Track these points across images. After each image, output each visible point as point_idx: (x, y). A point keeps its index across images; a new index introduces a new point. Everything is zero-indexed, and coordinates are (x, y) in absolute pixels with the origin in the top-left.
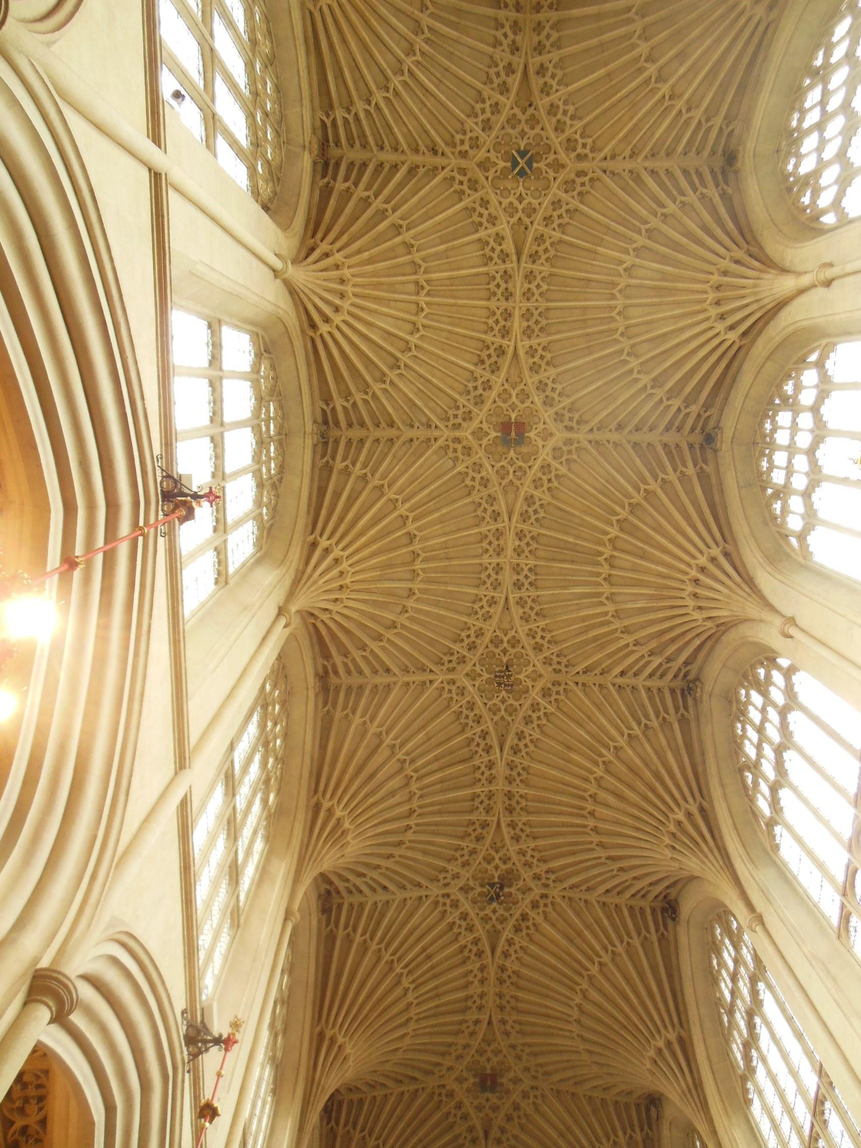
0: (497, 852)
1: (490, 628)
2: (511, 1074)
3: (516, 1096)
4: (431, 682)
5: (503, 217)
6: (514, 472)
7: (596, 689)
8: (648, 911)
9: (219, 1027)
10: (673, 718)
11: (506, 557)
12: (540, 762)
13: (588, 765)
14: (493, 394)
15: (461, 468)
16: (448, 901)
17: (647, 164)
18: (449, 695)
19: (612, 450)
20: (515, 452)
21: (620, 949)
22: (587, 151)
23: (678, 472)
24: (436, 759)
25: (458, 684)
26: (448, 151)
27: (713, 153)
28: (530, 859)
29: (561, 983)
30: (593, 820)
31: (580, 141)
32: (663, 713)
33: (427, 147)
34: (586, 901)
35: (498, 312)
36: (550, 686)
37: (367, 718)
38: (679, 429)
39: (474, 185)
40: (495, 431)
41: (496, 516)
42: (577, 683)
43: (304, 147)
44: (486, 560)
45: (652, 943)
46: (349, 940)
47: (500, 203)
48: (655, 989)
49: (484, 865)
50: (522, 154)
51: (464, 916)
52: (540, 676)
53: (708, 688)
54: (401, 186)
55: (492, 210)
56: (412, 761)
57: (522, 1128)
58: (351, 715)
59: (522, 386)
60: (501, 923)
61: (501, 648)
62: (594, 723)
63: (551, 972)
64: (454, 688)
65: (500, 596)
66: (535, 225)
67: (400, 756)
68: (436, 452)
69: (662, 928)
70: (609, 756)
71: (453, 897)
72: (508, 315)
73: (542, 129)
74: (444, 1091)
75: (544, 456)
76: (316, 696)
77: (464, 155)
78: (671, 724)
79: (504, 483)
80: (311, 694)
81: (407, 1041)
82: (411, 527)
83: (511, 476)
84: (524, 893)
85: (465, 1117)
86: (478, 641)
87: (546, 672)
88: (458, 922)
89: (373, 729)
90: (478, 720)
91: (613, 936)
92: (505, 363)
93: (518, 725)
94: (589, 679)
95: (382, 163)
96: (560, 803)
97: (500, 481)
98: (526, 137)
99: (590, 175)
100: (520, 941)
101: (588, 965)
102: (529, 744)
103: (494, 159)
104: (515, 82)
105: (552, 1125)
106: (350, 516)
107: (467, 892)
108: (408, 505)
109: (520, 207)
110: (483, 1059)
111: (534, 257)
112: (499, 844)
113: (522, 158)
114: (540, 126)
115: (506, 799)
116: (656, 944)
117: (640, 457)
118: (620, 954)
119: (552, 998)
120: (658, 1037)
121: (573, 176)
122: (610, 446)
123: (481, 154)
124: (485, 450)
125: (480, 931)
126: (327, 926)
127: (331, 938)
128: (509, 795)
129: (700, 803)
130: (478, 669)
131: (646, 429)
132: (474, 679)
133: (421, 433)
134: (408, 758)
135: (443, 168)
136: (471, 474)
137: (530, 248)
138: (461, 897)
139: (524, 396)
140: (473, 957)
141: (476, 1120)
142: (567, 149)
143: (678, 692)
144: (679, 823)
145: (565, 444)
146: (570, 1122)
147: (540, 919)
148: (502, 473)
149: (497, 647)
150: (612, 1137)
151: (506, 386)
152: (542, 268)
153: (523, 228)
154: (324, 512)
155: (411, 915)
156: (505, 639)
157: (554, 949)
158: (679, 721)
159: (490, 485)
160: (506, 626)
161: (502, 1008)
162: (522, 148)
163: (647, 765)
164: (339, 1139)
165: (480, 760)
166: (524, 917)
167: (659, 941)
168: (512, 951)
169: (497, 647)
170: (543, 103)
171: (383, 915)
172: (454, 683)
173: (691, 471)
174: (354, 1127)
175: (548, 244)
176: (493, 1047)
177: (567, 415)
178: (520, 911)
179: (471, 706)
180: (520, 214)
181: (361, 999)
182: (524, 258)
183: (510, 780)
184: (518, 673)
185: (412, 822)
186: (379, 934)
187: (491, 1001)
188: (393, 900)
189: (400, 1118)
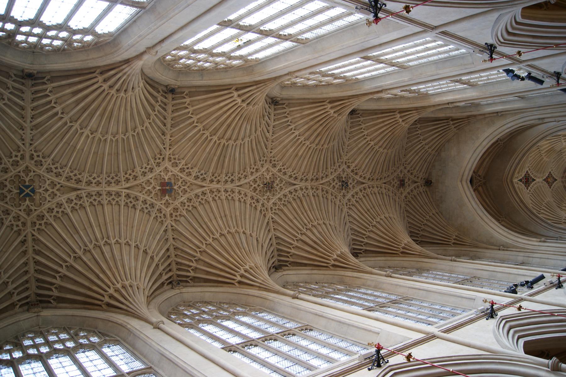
0: (331, 184)
1: (250, 193)
2: (400, 174)
4: (272, 219)
5: (57, 200)
6: (183, 186)
7: (274, 144)
8: (352, 120)
9: (488, 305)
10: (288, 110)
11: (220, 188)
12: (301, 168)
13: (304, 148)
14: (149, 198)
15: (184, 212)
16: (348, 203)
17: (28, 121)
18: (277, 210)
19: (174, 138)
20: (175, 186)
21: (366, 133)
22: (19, 154)
23: (188, 107)
24: (303, 214)
25: (272, 206)
26: (23, 234)
27: (23, 84)
28: (334, 170)
29: (375, 156)
30: (324, 145)
31: (14, 158)
32: (286, 115)
33: (22, 246)
34: (348, 146)
35: (108, 199)
36: (271, 164)
37: (291, 246)
38: (166, 105)
39: (42, 217)
40: (165, 196)
41: (204, 194)
42: (271, 152)
43: (37, 316)
44: (223, 197)
45: (364, 120)
46: (367, 244)
47: (49, 201)
48: (381, 120)
49: (336, 189)
50: (22, 191)
52: (267, 169)
53: (278, 95)
54: (48, 258)
55: (54, 206)
56: (305, 225)
57: (414, 169)
58: (290, 254)
59: (144, 184)
60: (354, 180)
61: (257, 187)
62: (287, 145)
63: (371, 160)
64: (274, 208)
66: (61, 182)
67: (305, 230)
68: (178, 225)
69: (359, 115)
70: (302, 138)
71: (347, 202)
72: (109, 194)
73: (6, 180)
74: (405, 200)
75: (176, 172)
76: (284, 270)
77: (24, 224)
78: (290, 111)
79: (189, 191)
80: (285, 273)
81: (396, 217)
82: (217, 235)
83: (186, 187)
84: (344, 172)
85: (412, 191)
86: (255, 198)
88: (355, 199)
89: (295, 243)
90: (285, 196)
91: (361, 135)
92: (133, 193)
93: (286, 178)
94: (270, 146)
95: (35, 270)
96: (317, 159)
97: (188, 192)
98: (11, 189)
99: (33, 152)
101: (370, 145)
102: (293, 173)
103: (25, 207)
105: (414, 157)
106: (220, 266)
107: (345, 196)
108: (208, 238)
109: (51, 190)
110: (396, 185)
111: (78, 181)
112: (328, 183)
113: (25, 191)
114: (4, 182)
115: (313, 181)
116: (364, 118)
117: (179, 125)
118: (368, 133)
119: (379, 160)
120: (398, 121)
121: (33, 162)
122: (172, 139)
123: (22, 214)
124: (174, 201)
125: (357, 189)
126: (362, 254)
127: (366, 251)
128: (312, 180)
129: (327, 103)
130: (265, 197)
131: (165, 121)
132: (269, 199)
133: (170, 233)
134: (305, 227)
135: (33, 235)
136: (186, 207)
137: (73, 184)
138: (347, 198)
139: (148, 182)
140: (366, 192)
142: (18, 165)
143: (276, 107)
144: (334, 112)
145: (171, 161)
146: (414, 151)
147: (354, 165)
148: (185, 191)
149: (257, 189)
150: (419, 135)
151: (144, 192)
152: (85, 177)
153: (62, 188)
154: (220, 279)
155: (355, 219)
156: (254, 186)
157: (364, 159)
158: (290, 108)
159: (190, 198)
160: (248, 186)
161: (381, 179)
162: (18, 191)
163: (308, 123)
164: (423, 240)
165: (300, 193)
166: (352, 171)
167: (363, 117)
168: (364, 176)
169: (257, 189)
171: (356, 230)
172: (271, 208)
173: (188, 100)
174: (419, 234)
175: (71, 174)
176: (392, 182)
177: (158, 161)
178: (351, 173)
179: (280, 199)
180: (55, 190)
181: (388, 238)
182: (79, 187)
183: (307, 180)
184: (266, 178)
185: (327, 222)
186: (363, 232)
187: (379, 183)
188: (350, 227)
189: (414, 216)
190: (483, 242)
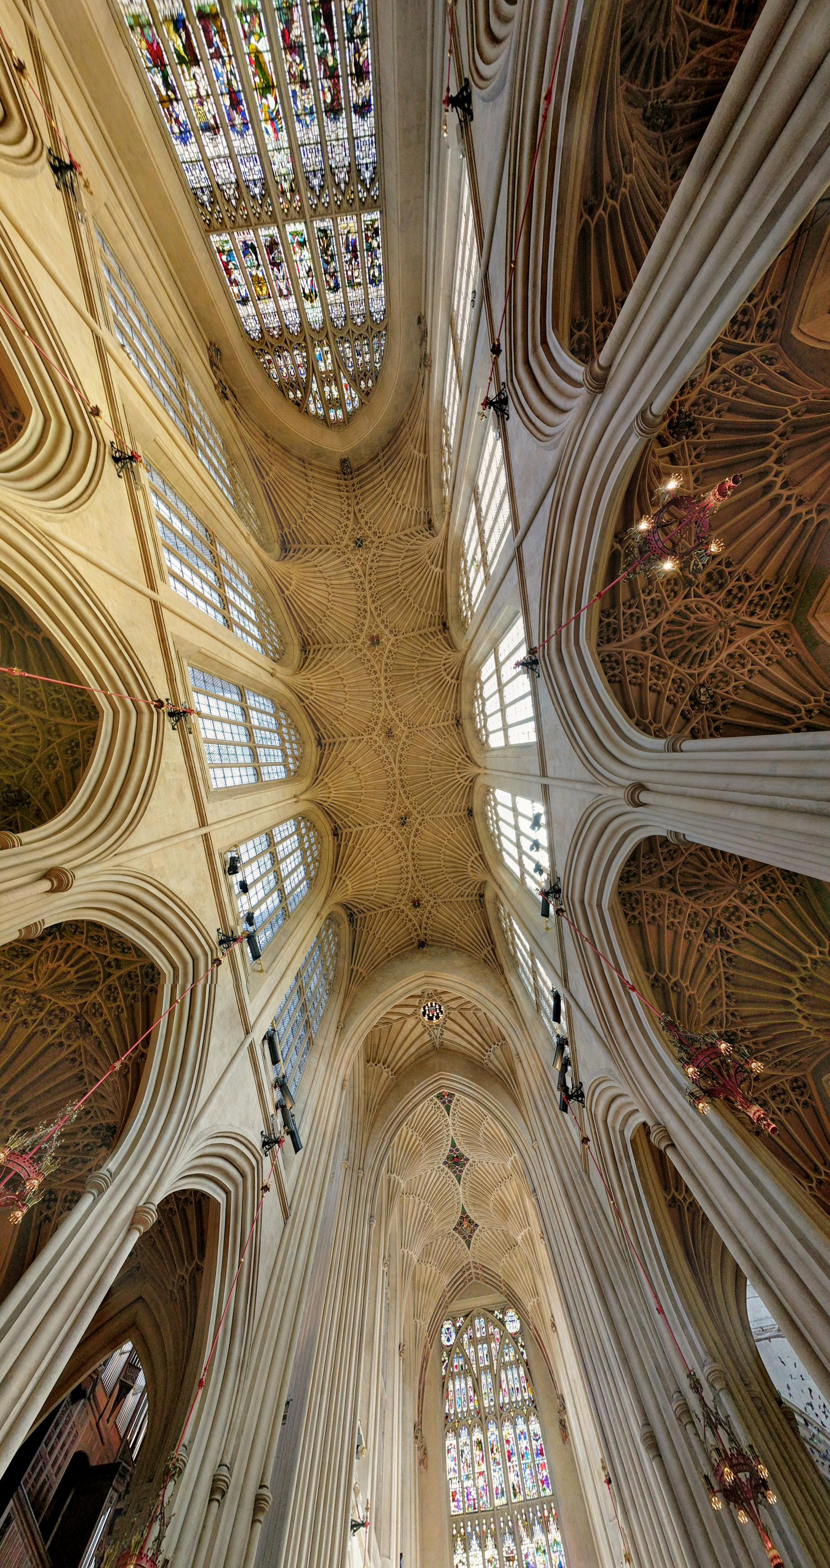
1: (381, 715)
3: (429, 908)
39: (344, 553)
51: (394, 834)
65: (382, 702)
87: (405, 729)
89: (340, 756)
92: (368, 615)
100: (418, 840)
104: (351, 516)
123: (345, 543)
125: (401, 839)
127: (339, 845)
128: (402, 780)
139: (377, 626)
141: (415, 921)
170: (362, 521)
190: (352, 1004)
